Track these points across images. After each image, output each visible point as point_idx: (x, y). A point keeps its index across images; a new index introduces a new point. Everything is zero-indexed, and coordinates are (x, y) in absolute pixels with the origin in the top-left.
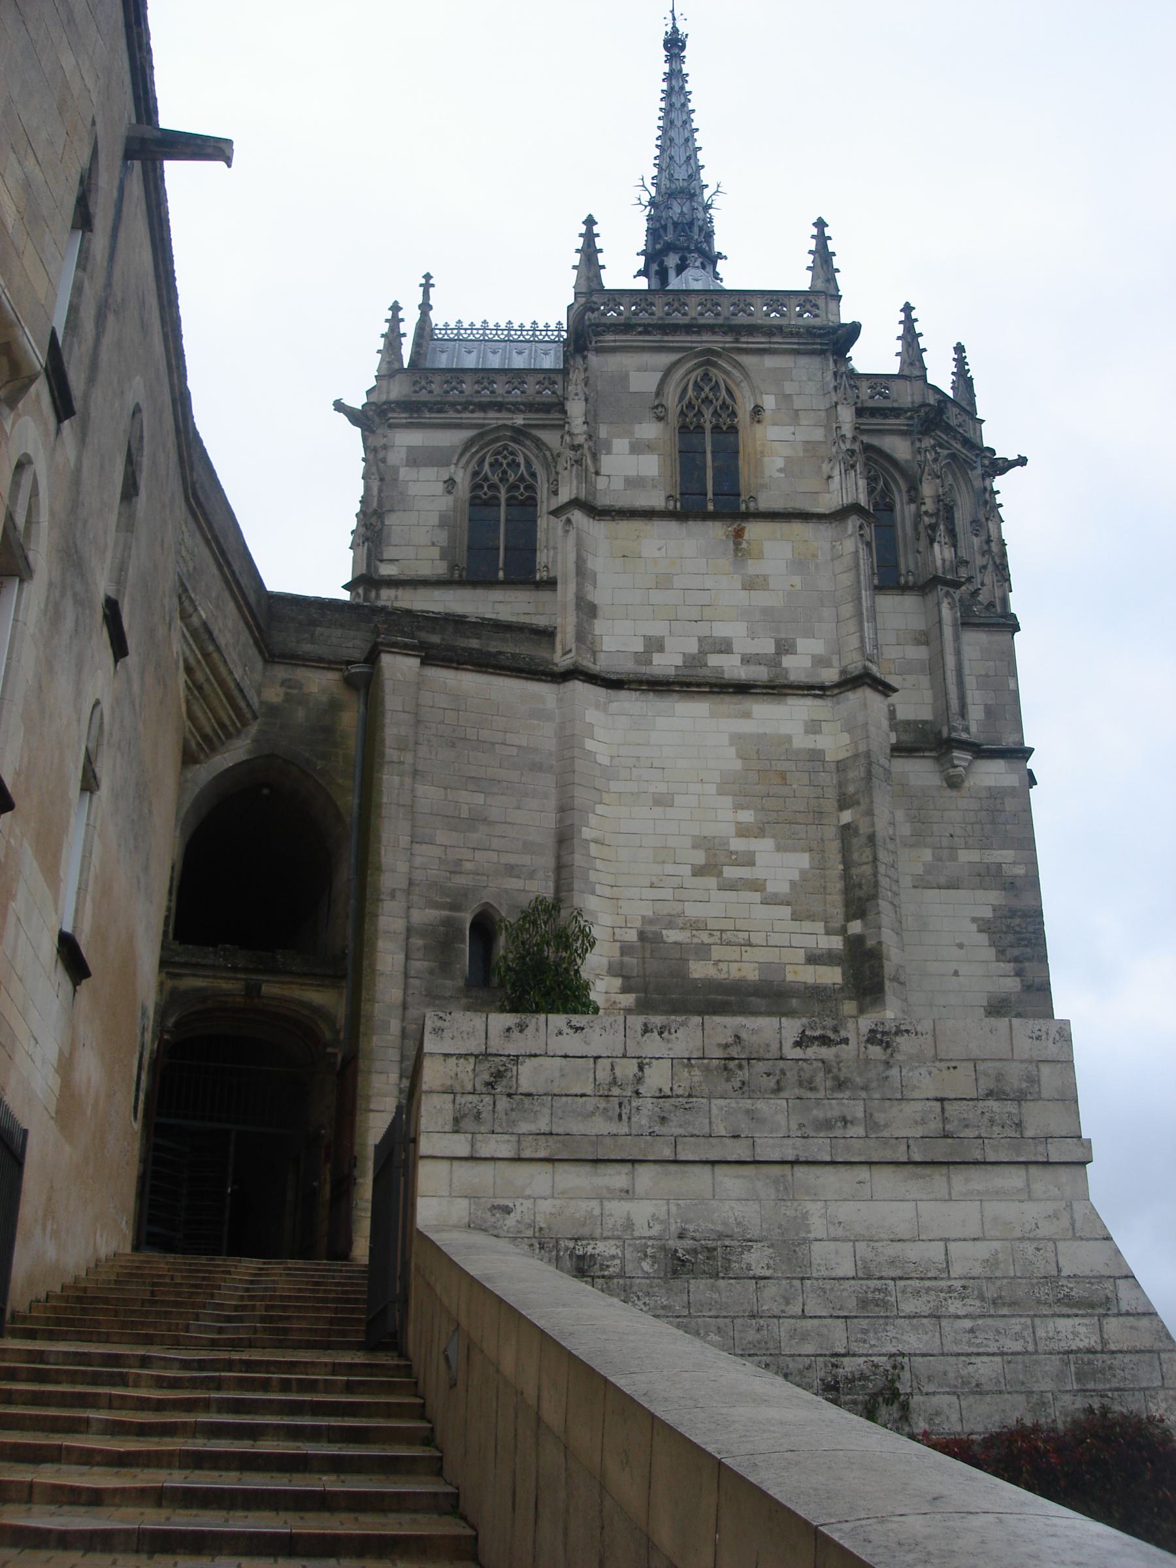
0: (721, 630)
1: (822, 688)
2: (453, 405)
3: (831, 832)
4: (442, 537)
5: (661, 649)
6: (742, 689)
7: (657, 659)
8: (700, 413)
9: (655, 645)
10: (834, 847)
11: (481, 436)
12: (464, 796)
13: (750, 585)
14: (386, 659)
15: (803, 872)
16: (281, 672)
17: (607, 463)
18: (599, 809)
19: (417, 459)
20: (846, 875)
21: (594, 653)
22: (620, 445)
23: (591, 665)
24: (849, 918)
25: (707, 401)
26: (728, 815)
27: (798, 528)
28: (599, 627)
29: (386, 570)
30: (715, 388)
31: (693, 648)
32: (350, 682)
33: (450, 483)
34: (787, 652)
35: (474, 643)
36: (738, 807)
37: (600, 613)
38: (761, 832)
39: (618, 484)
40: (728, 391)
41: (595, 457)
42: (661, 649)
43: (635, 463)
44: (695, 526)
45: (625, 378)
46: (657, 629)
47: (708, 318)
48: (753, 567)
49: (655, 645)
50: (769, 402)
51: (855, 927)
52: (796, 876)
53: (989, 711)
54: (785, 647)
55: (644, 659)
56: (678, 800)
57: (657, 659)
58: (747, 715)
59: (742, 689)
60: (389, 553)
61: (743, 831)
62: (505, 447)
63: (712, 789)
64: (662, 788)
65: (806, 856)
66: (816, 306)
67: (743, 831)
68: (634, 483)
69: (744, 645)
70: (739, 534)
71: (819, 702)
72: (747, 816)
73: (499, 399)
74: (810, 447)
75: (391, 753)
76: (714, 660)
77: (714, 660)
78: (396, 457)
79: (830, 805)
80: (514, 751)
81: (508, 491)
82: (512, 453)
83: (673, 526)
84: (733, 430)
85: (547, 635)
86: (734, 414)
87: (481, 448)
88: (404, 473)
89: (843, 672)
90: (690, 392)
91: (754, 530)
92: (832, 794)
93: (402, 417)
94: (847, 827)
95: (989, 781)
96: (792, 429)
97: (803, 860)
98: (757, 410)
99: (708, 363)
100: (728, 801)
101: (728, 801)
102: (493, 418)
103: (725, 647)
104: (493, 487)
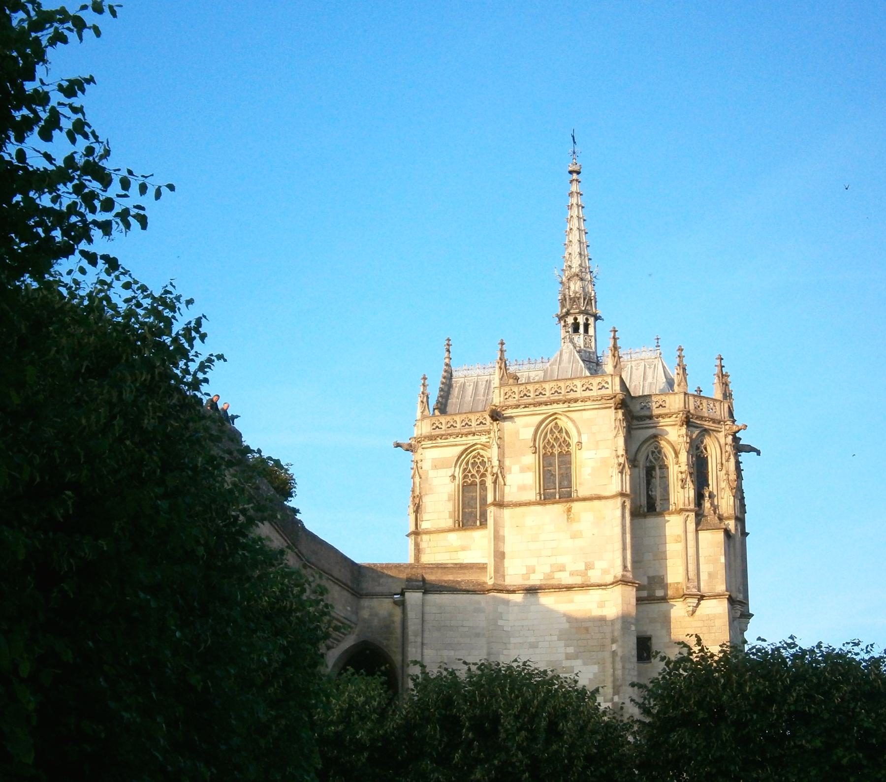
0: (561, 560)
1: (606, 585)
2: (450, 435)
3: (607, 655)
4: (450, 507)
5: (534, 572)
6: (569, 588)
7: (532, 577)
8: (553, 446)
9: (532, 570)
10: (609, 660)
11: (466, 450)
12: (445, 653)
13: (574, 537)
14: (408, 595)
15: (594, 674)
16: (365, 602)
17: (509, 479)
18: (505, 652)
19: (438, 465)
20: (614, 675)
21: (504, 576)
22: (515, 468)
23: (502, 583)
24: (614, 694)
25: (556, 439)
26: (562, 650)
27: (596, 502)
28: (507, 562)
29: (424, 525)
30: (561, 431)
31: (547, 570)
32: (396, 603)
33: (454, 477)
34: (590, 568)
35: (450, 577)
36: (566, 646)
37: (506, 556)
38: (576, 656)
39: (514, 489)
40: (567, 433)
41: (504, 477)
42: (534, 572)
43: (521, 477)
44: (550, 507)
45: (517, 433)
46: (532, 562)
47: (556, 397)
48: (576, 526)
49: (532, 570)
50: (584, 439)
51: (616, 699)
52: (591, 676)
53: (710, 575)
54: (589, 566)
55: (526, 576)
56: (541, 645)
57: (532, 577)
58: (571, 601)
59: (569, 588)
60: (425, 516)
61: (568, 657)
62: (479, 453)
63: (555, 638)
64: (533, 640)
65: (596, 667)
66: (607, 383)
67: (568, 657)
68: (522, 488)
69: (569, 568)
70: (569, 510)
71: (604, 591)
72: (571, 650)
73: (473, 430)
74: (604, 461)
75: (411, 638)
76: (558, 575)
77: (558, 575)
78: (426, 465)
79: (608, 641)
80: (467, 629)
81: (481, 477)
82: (482, 456)
83: (539, 508)
84: (568, 453)
85: (482, 568)
86: (568, 445)
87: (467, 455)
88: (432, 474)
89: (615, 577)
90: (549, 436)
91: (576, 506)
92: (609, 636)
93: (427, 443)
94: (614, 651)
95: (708, 611)
96: (594, 452)
97: (595, 669)
98: (579, 443)
99: (556, 418)
100: (562, 643)
101: (562, 643)
102: (471, 440)
103: (562, 569)
104: (472, 476)
